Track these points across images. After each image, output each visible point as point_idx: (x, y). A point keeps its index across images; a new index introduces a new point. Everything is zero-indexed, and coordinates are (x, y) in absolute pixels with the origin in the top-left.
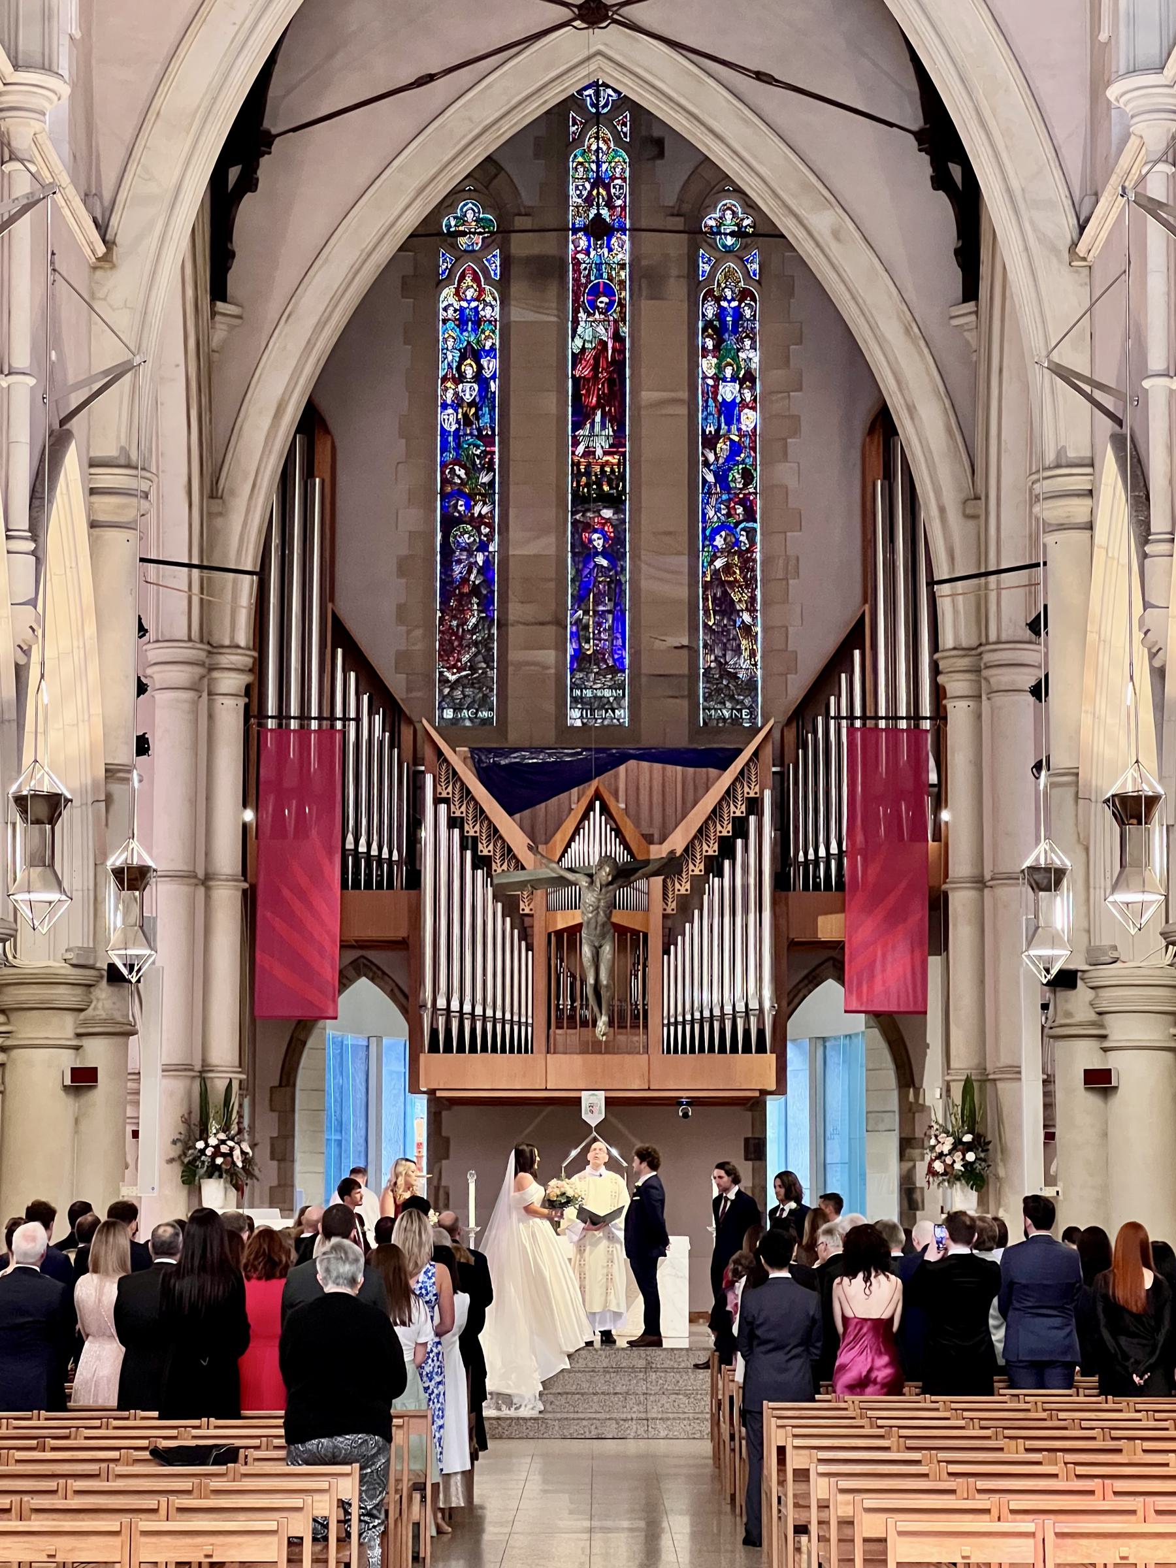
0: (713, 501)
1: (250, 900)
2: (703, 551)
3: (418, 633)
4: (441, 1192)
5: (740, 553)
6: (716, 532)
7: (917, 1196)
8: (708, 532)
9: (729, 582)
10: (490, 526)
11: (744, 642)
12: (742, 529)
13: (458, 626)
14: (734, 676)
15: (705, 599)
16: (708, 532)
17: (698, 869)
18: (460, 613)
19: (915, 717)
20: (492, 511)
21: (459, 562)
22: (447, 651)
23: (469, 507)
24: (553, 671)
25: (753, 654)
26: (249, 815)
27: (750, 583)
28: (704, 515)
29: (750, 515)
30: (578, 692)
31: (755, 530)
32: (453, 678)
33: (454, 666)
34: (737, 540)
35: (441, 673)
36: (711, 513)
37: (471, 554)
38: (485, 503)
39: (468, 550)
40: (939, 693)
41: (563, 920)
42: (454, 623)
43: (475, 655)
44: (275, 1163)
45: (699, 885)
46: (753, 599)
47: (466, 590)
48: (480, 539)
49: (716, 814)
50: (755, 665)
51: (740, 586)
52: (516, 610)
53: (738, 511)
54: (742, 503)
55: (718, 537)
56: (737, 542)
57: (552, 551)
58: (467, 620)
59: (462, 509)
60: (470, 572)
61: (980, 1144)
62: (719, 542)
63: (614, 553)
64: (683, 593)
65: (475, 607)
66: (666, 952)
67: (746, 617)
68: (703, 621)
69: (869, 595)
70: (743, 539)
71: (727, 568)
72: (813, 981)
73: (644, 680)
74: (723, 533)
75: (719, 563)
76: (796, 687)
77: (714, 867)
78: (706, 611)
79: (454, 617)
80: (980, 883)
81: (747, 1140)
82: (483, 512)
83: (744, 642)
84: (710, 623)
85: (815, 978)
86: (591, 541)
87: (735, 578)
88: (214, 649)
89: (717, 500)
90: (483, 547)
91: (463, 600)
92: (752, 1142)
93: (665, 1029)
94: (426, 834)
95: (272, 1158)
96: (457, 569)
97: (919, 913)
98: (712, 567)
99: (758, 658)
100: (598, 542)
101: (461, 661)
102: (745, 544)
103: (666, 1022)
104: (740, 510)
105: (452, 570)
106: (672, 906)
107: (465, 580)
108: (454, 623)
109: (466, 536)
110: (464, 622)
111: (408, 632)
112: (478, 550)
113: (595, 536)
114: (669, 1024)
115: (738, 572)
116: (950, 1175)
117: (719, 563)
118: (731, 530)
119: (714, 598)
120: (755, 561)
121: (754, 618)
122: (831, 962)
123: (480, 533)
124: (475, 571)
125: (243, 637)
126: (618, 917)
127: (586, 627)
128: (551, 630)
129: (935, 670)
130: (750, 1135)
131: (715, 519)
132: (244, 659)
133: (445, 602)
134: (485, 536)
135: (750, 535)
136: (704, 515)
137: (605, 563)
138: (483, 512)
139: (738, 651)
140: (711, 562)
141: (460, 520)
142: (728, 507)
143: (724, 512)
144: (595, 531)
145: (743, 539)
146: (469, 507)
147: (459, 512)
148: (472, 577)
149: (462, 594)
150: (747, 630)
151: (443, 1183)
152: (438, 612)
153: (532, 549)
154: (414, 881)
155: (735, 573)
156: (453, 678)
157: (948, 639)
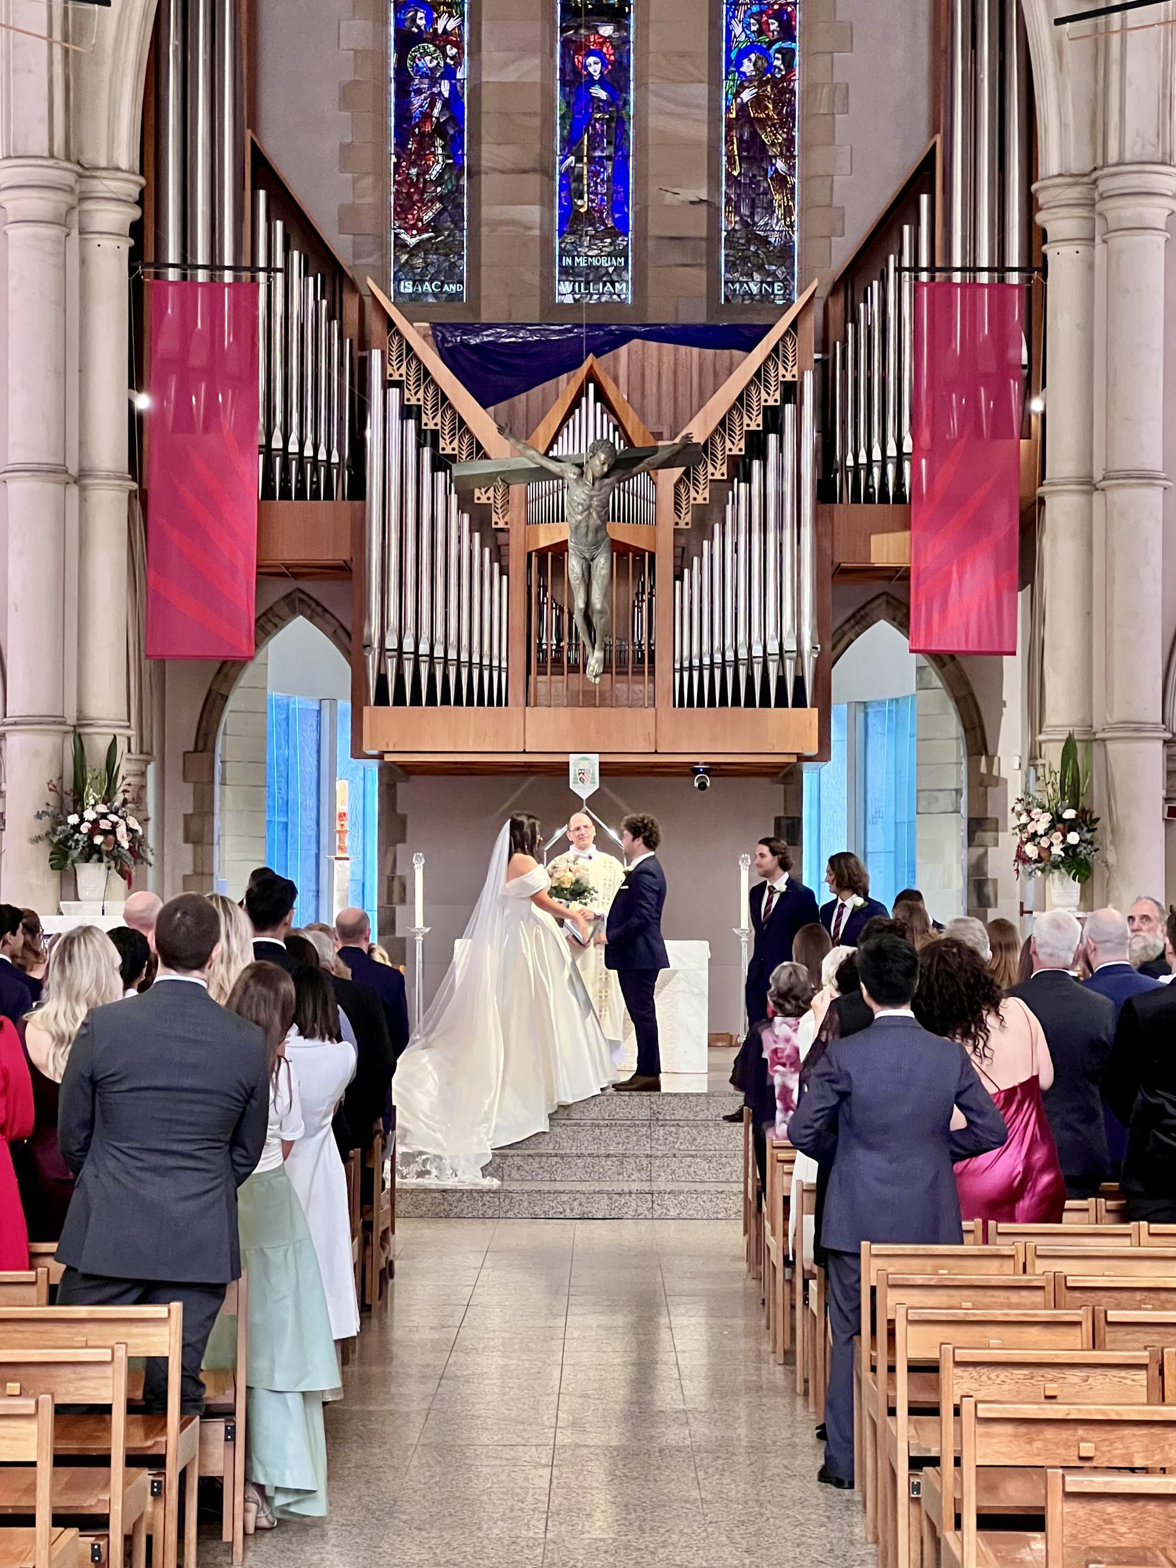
0: (741, 15)
1: (141, 500)
2: (727, 79)
3: (368, 181)
4: (396, 883)
5: (775, 82)
6: (744, 54)
7: (989, 889)
8: (733, 56)
9: (759, 120)
10: (458, 45)
11: (777, 197)
12: (777, 51)
13: (418, 175)
14: (765, 241)
15: (729, 142)
16: (733, 56)
17: (720, 471)
18: (420, 157)
19: (1000, 268)
20: (460, 27)
21: (419, 92)
22: (403, 209)
23: (430, 21)
24: (537, 232)
25: (788, 211)
26: (143, 402)
27: (787, 121)
28: (729, 32)
29: (787, 32)
30: (569, 261)
31: (793, 51)
32: (412, 242)
33: (414, 226)
34: (771, 64)
35: (396, 235)
36: (737, 29)
37: (434, 82)
38: (451, 16)
39: (432, 77)
40: (1034, 236)
41: (547, 536)
42: (414, 171)
43: (440, 213)
44: (190, 846)
45: (720, 490)
46: (790, 141)
47: (428, 128)
48: (445, 63)
49: (742, 400)
50: (791, 226)
51: (774, 125)
52: (490, 154)
53: (772, 27)
54: (777, 16)
55: (745, 61)
56: (771, 68)
57: (536, 77)
58: (429, 167)
59: (422, 23)
60: (432, 106)
61: (1085, 821)
62: (747, 67)
63: (616, 80)
64: (701, 132)
65: (440, 151)
66: (679, 577)
67: (780, 165)
68: (727, 170)
69: (940, 121)
70: (777, 63)
71: (758, 101)
72: (860, 621)
73: (651, 244)
74: (753, 56)
75: (746, 96)
76: (843, 250)
77: (740, 469)
78: (730, 159)
79: (413, 164)
80: (1089, 485)
81: (778, 820)
82: (449, 28)
83: (777, 197)
84: (735, 173)
85: (863, 617)
86: (586, 67)
87: (767, 115)
88: (85, 171)
89: (745, 12)
90: (449, 73)
91: (425, 143)
92: (784, 822)
93: (677, 675)
94: (373, 434)
95: (186, 840)
96: (417, 101)
97: (1005, 520)
98: (739, 100)
99: (795, 218)
100: (594, 67)
101: (421, 220)
102: (780, 70)
103: (677, 666)
104: (774, 25)
105: (410, 103)
106: (686, 519)
107: (427, 116)
108: (414, 171)
109: (428, 58)
110: (426, 170)
111: (355, 181)
112: (442, 77)
113: (591, 60)
114: (682, 669)
115: (771, 106)
116: (1045, 862)
117: (746, 96)
118: (764, 52)
119: (740, 140)
120: (793, 92)
121: (792, 168)
122: (884, 598)
123: (445, 55)
124: (439, 105)
125: (126, 153)
126: (620, 532)
127: (579, 178)
128: (534, 180)
129: (1030, 204)
130: (782, 814)
131: (743, 36)
132: (130, 187)
133: (401, 144)
134: (452, 58)
135: (788, 56)
136: (729, 32)
137: (603, 95)
138: (449, 28)
139: (769, 209)
140: (737, 95)
141: (419, 38)
142: (759, 22)
143: (754, 28)
144: (590, 53)
145: (777, 63)
146: (430, 21)
147: (418, 27)
148: (436, 112)
149: (422, 134)
150: (781, 181)
151: (398, 873)
152: (393, 157)
153: (510, 75)
154: (358, 490)
155: (767, 108)
156: (412, 242)
157: (1051, 161)
